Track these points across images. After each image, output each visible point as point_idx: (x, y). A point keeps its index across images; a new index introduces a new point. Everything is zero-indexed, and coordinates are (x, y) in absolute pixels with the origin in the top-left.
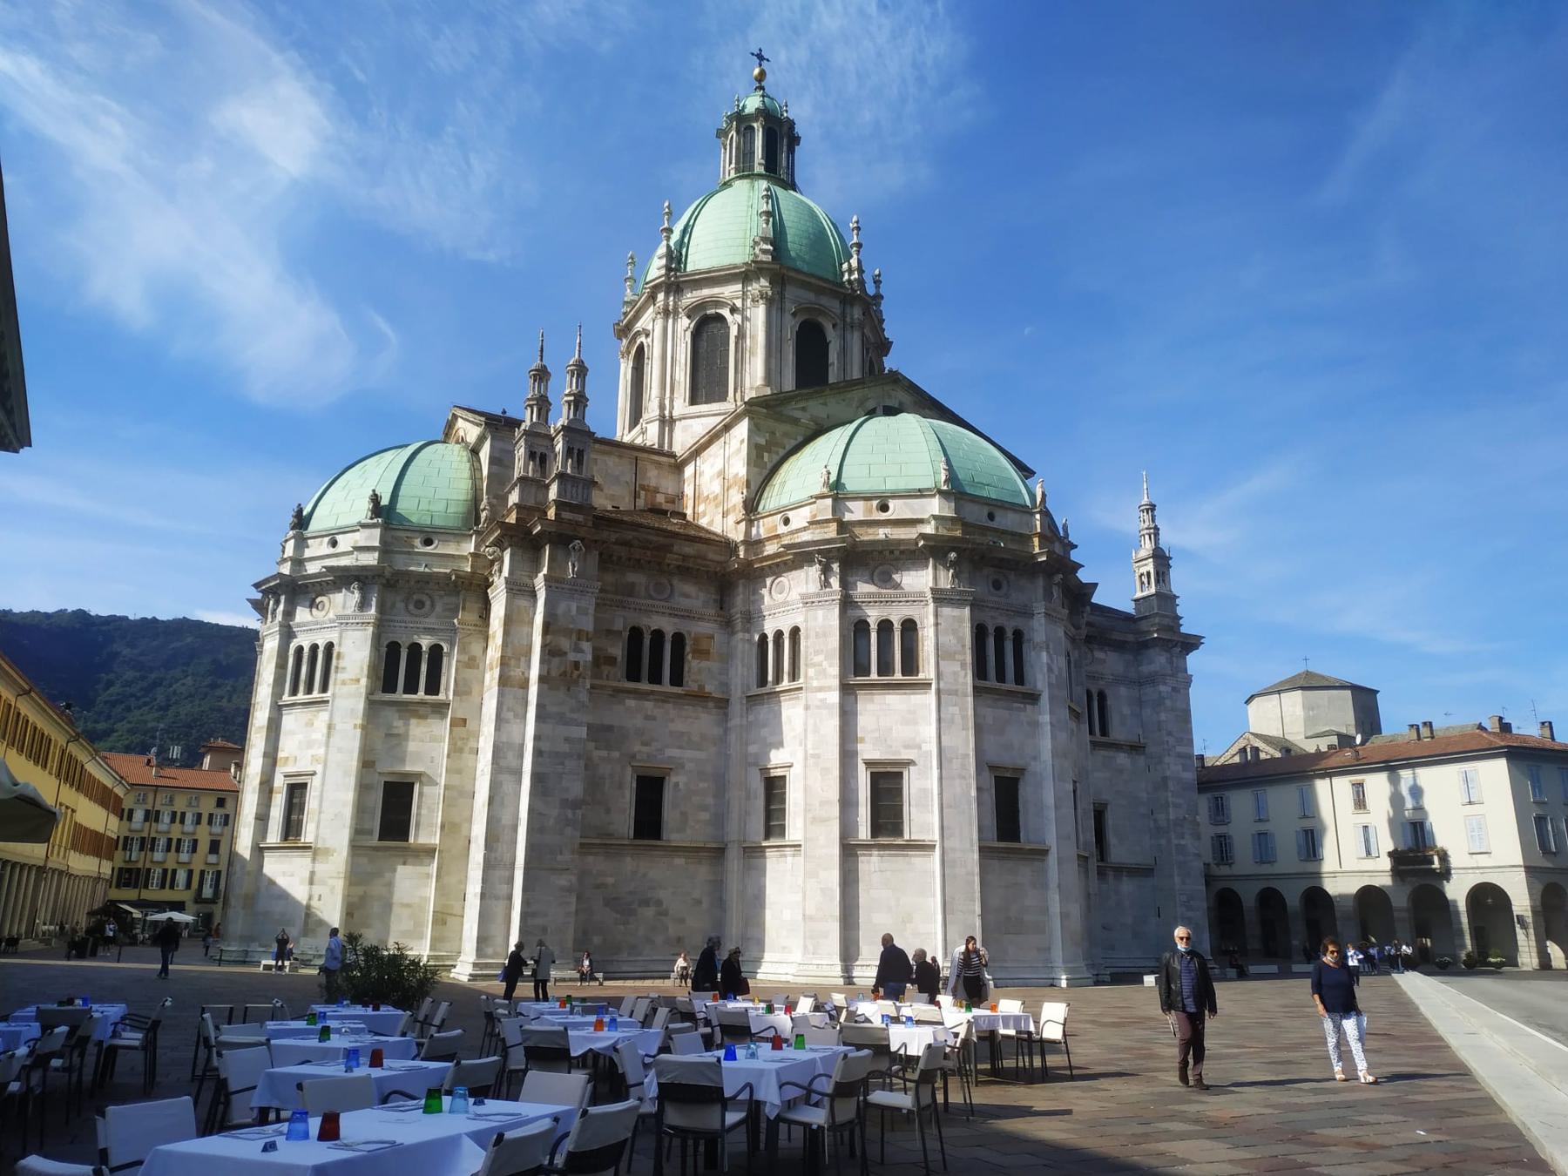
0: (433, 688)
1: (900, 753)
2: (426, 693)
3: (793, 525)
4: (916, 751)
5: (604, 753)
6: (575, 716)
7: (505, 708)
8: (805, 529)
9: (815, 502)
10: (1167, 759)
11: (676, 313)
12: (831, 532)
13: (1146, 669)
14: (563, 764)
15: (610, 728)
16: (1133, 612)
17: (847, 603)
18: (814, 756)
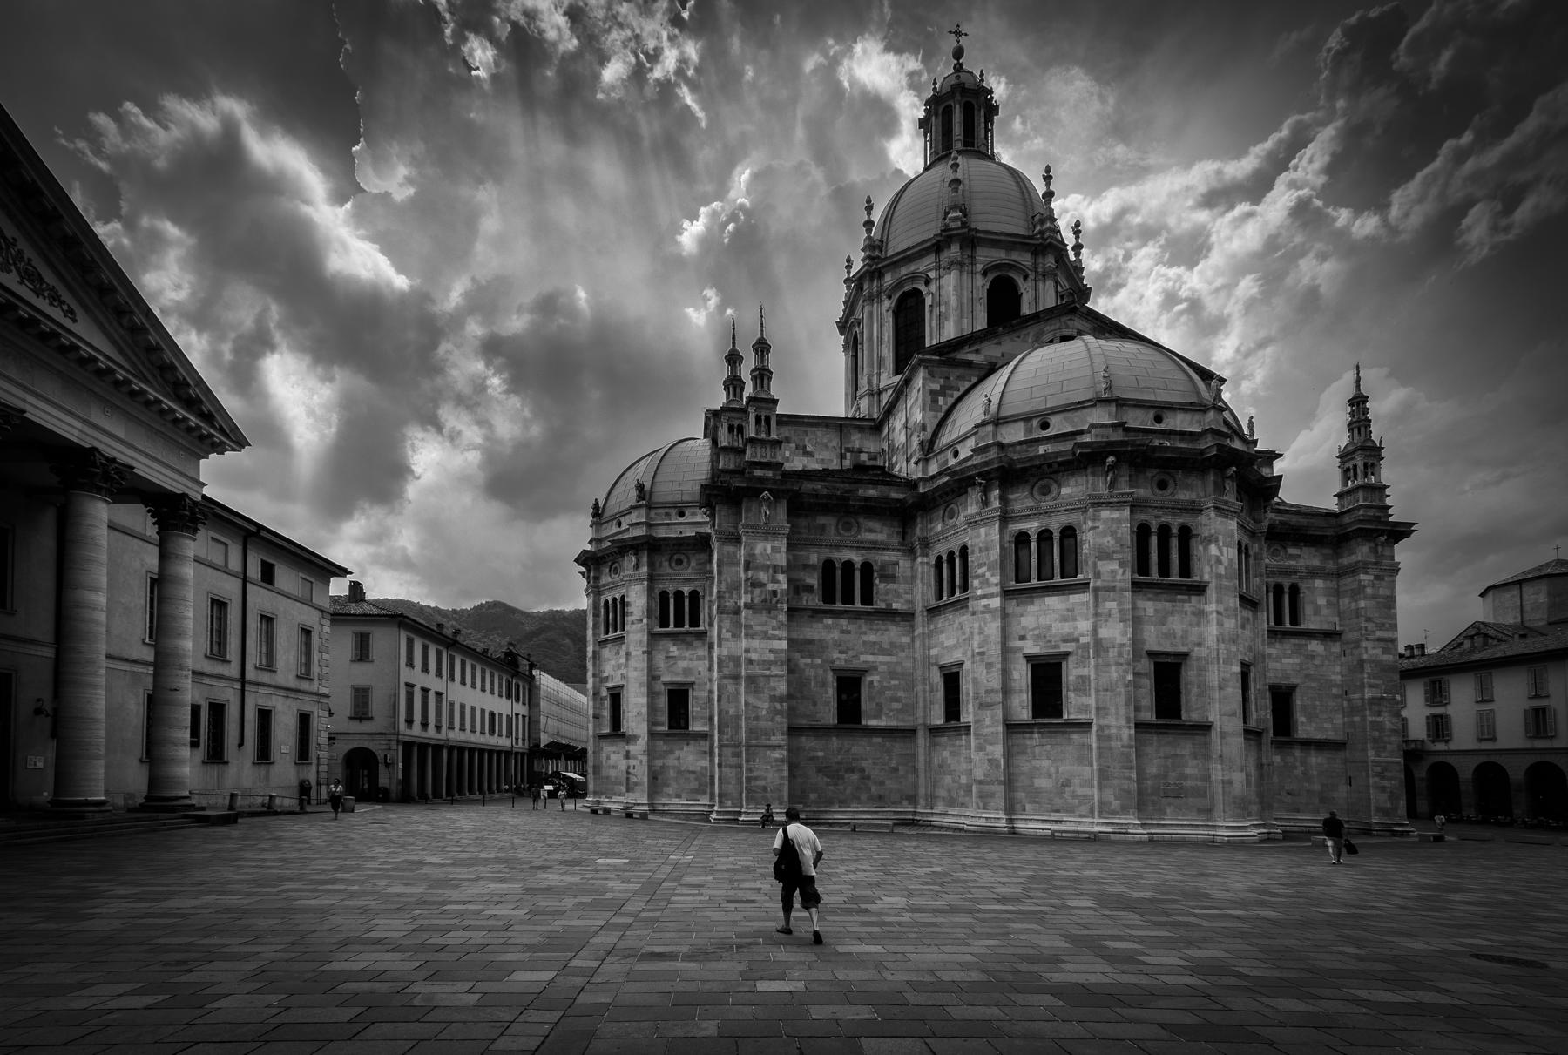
0: (695, 622)
1: (1058, 647)
2: (690, 626)
3: (962, 456)
4: (1073, 644)
5: (809, 661)
6: (776, 632)
7: (724, 630)
8: (970, 458)
9: (977, 432)
10: (1364, 644)
11: (879, 293)
12: (993, 454)
13: (1345, 561)
14: (769, 669)
15: (811, 642)
16: (1336, 508)
17: (1005, 518)
18: (980, 654)
